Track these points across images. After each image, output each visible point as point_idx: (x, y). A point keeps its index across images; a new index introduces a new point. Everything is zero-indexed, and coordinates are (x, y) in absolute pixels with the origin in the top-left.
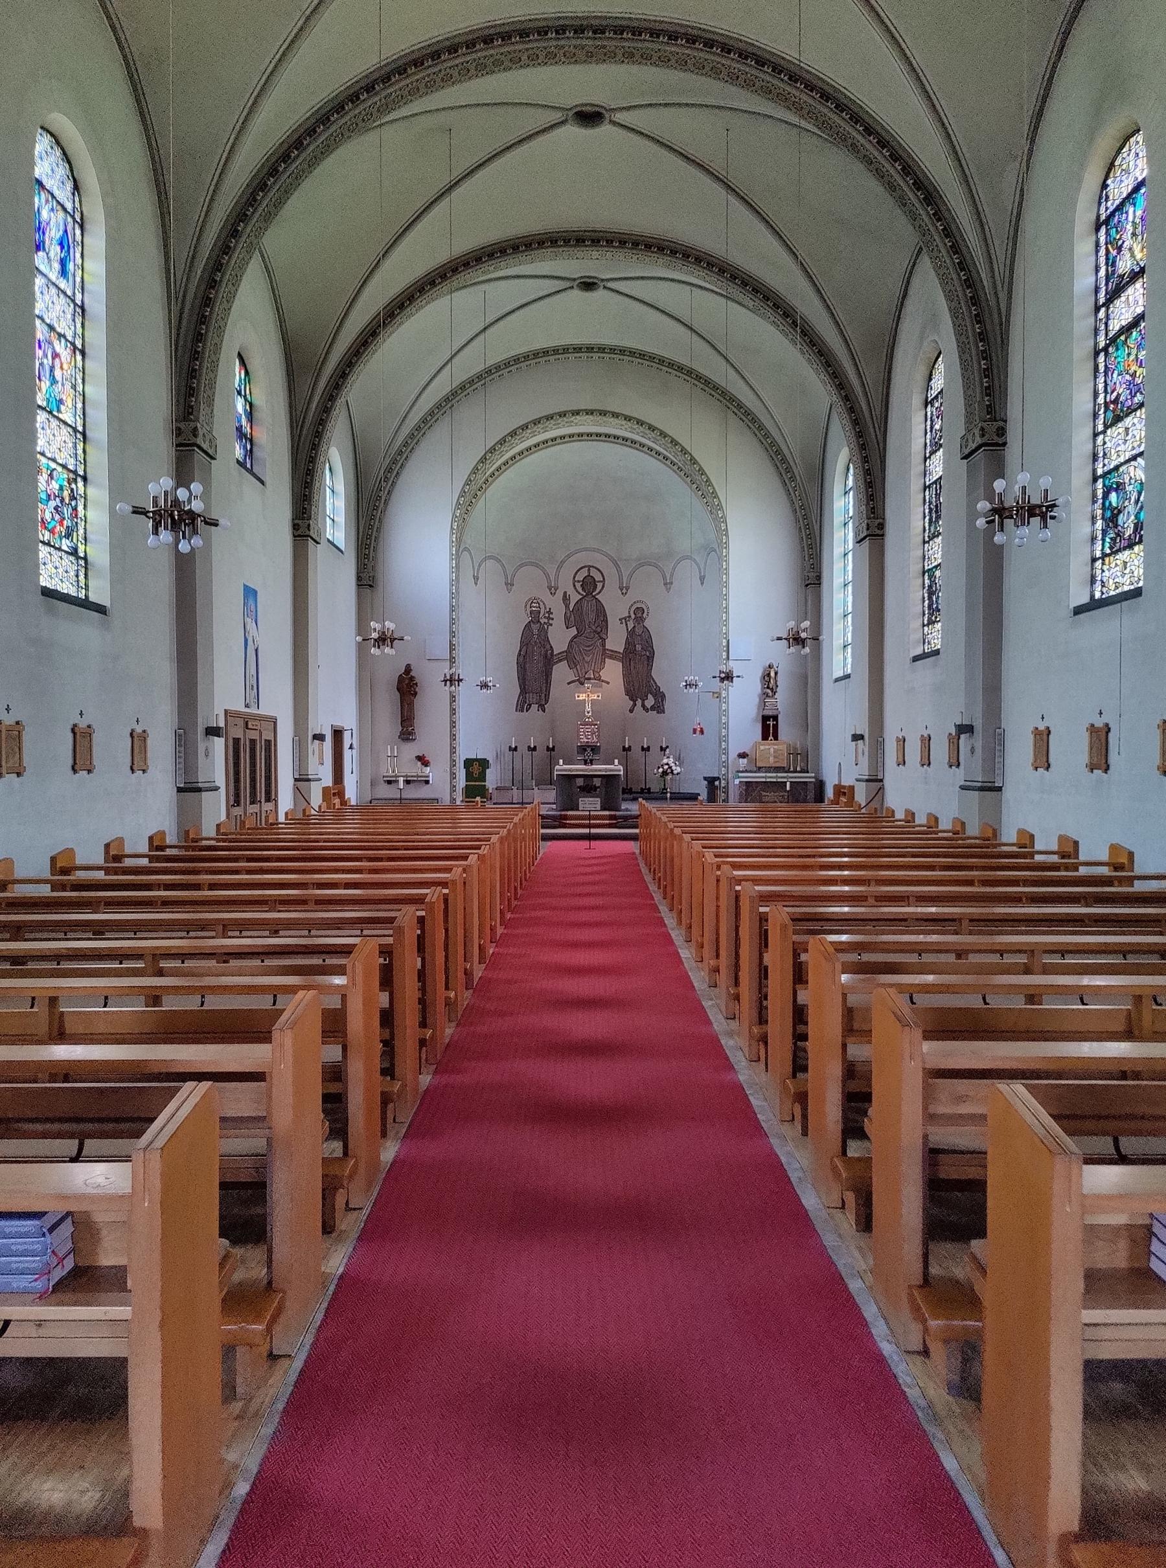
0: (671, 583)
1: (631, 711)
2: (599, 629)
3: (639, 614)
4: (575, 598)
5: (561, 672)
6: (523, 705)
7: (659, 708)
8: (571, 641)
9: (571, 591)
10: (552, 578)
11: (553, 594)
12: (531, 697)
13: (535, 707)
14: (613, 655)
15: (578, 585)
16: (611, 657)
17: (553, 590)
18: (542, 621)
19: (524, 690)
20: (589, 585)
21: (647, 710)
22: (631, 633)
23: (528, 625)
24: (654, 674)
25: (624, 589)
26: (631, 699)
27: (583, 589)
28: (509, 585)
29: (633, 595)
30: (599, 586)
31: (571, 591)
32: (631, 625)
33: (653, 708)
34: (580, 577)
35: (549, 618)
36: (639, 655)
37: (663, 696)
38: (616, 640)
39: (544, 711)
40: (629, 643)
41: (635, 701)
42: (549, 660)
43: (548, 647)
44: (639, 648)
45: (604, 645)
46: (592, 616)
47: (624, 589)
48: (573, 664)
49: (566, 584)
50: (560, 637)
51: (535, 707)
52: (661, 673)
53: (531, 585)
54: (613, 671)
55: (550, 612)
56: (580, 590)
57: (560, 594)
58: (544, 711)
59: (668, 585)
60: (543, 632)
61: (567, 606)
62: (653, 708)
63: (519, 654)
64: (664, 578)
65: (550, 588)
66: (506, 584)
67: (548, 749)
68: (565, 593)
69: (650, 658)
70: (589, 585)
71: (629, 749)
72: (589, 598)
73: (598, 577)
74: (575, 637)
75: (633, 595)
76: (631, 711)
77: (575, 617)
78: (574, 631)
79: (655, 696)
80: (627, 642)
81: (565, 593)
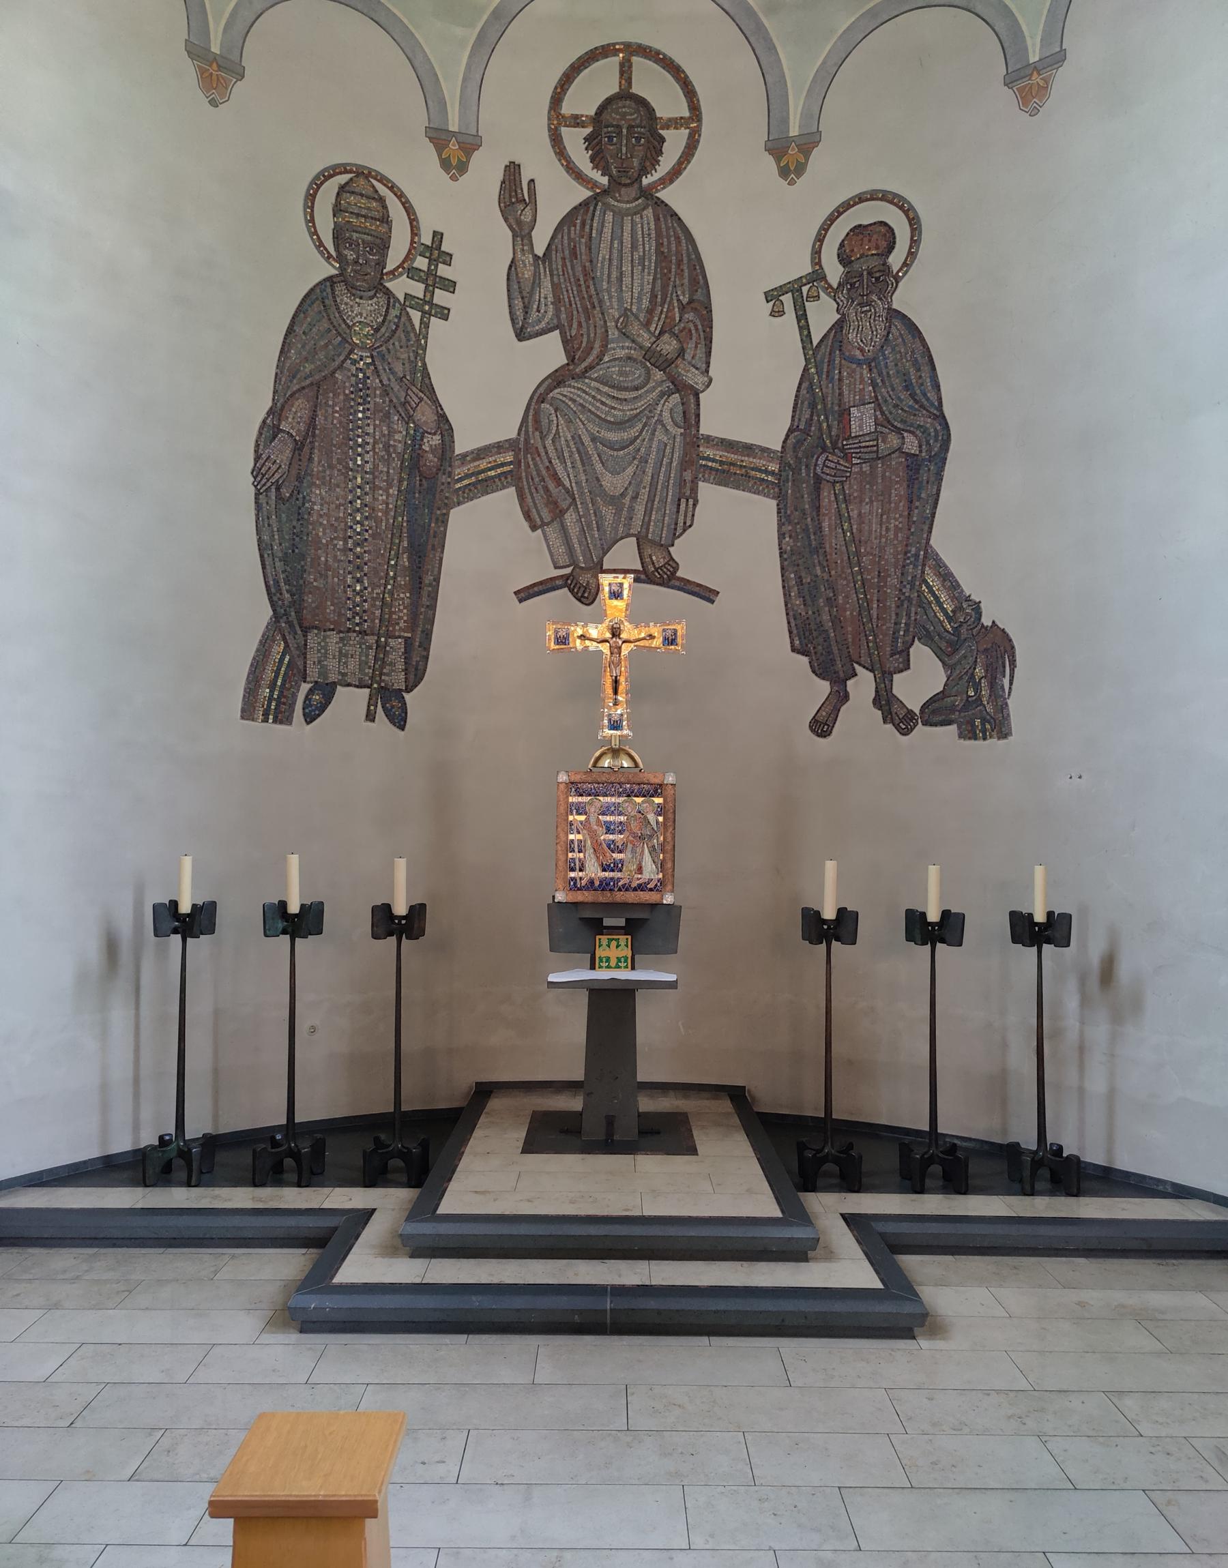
0: (1059, 58)
1: (822, 726)
2: (668, 346)
3: (868, 261)
4: (557, 197)
5: (487, 541)
6: (283, 687)
7: (975, 707)
8: (539, 397)
9: (541, 168)
10: (451, 90)
11: (455, 167)
12: (327, 651)
13: (350, 701)
14: (736, 466)
15: (575, 140)
16: (727, 476)
17: (454, 150)
18: (401, 287)
19: (294, 608)
20: (627, 141)
21: (903, 721)
22: (824, 358)
23: (318, 300)
24: (945, 540)
25: (790, 155)
26: (822, 670)
27: (598, 160)
28: (217, 72)
29: (832, 176)
30: (675, 141)
31: (541, 168)
32: (823, 314)
33: (936, 712)
34: (586, 98)
35: (433, 281)
36: (872, 437)
37: (998, 650)
38: (752, 387)
39: (399, 720)
40: (816, 405)
41: (838, 678)
42: (431, 482)
43: (425, 415)
44: (863, 420)
45: (691, 418)
46: (638, 286)
47: (790, 155)
48: (545, 508)
49: (515, 128)
50: (483, 373)
51: (350, 701)
52: (979, 537)
53: (348, 96)
54: (736, 535)
55: (437, 252)
56: (581, 158)
57: (485, 173)
58: (399, 720)
59: (1029, 81)
60: (402, 338)
61: (521, 233)
62: (936, 712)
63: (270, 430)
64: (1010, 40)
65: (438, 137)
66: (197, 51)
67: (386, 923)
68: (513, 170)
69: (924, 471)
70: (627, 141)
71: (841, 928)
72: (624, 201)
73: (666, 101)
74: (557, 379)
75: (832, 176)
76: (822, 726)
77: (555, 287)
78: (549, 353)
79: (946, 652)
80: (808, 397)
81: (513, 170)
